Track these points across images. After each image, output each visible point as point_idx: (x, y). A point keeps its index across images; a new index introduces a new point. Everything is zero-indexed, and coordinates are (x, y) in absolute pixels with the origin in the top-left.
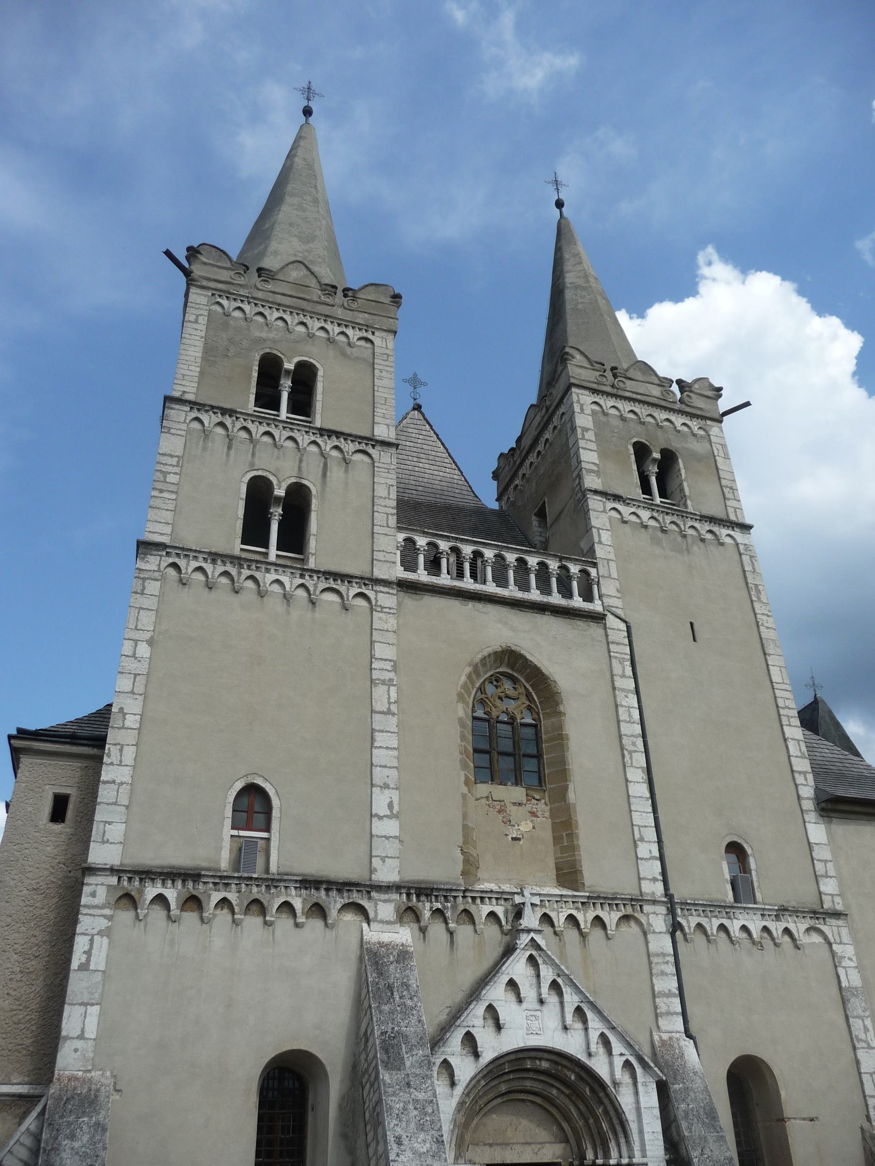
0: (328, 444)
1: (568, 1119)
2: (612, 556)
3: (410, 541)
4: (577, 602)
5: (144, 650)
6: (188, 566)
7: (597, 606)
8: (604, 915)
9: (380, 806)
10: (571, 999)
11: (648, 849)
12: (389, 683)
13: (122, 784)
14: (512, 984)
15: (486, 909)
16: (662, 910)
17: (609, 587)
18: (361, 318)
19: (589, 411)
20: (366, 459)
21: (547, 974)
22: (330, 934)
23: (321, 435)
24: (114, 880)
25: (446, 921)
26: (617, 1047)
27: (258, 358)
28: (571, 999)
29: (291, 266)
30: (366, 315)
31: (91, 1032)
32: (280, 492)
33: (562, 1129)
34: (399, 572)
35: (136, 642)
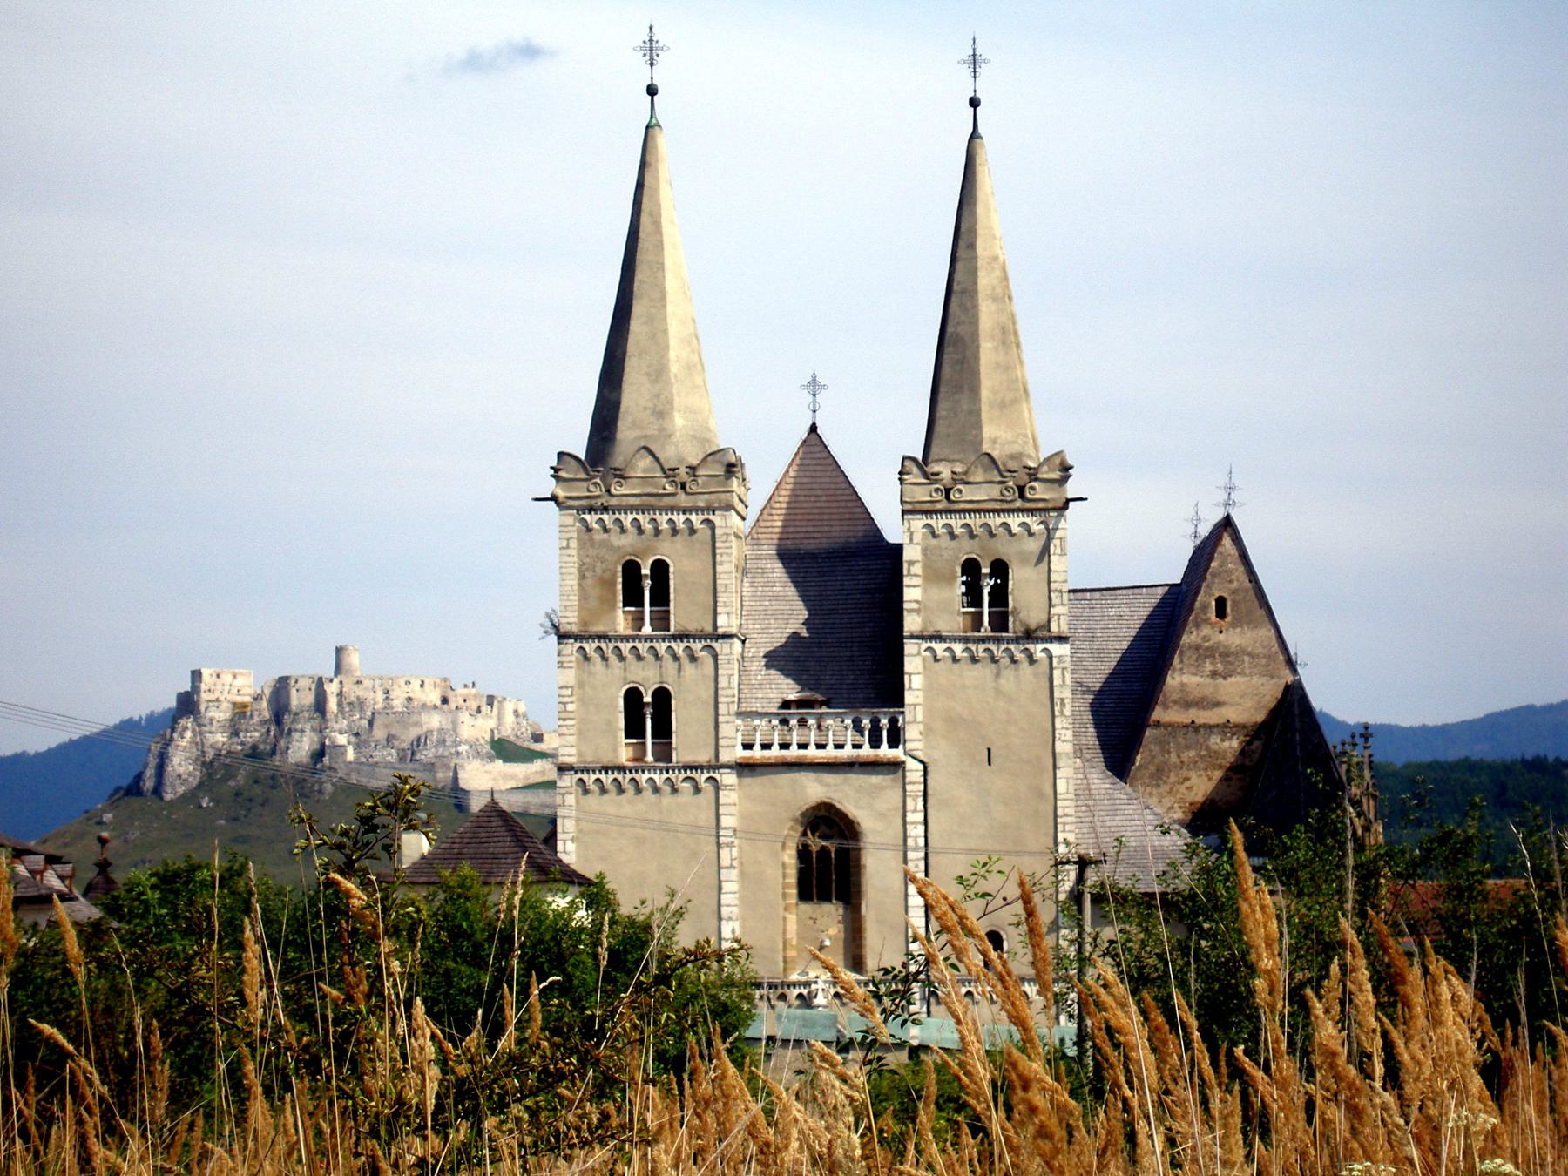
0: (679, 647)
2: (920, 700)
4: (885, 751)
6: (590, 779)
7: (897, 753)
15: (796, 992)
17: (912, 733)
19: (918, 538)
27: (620, 568)
29: (638, 456)
30: (706, 496)
32: (648, 699)
34: (740, 754)
35: (565, 841)
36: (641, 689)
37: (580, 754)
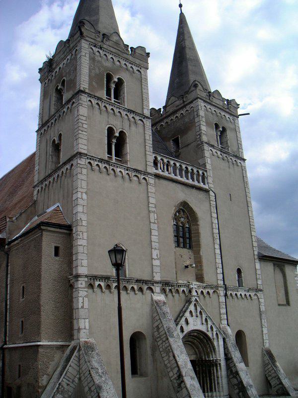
0: (131, 116)
1: (198, 348)
3: (156, 158)
4: (202, 185)
5: (85, 196)
6: (94, 163)
7: (206, 187)
8: (209, 290)
9: (154, 256)
10: (204, 316)
11: (220, 271)
12: (154, 212)
13: (84, 246)
14: (191, 312)
16: (222, 289)
17: (210, 180)
18: (137, 62)
20: (141, 123)
21: (199, 309)
22: (144, 297)
23: (128, 112)
24: (86, 279)
25: (172, 293)
26: (215, 329)
28: (204, 316)
31: (87, 327)
33: (195, 351)
36: (114, 128)
37: (88, 150)
